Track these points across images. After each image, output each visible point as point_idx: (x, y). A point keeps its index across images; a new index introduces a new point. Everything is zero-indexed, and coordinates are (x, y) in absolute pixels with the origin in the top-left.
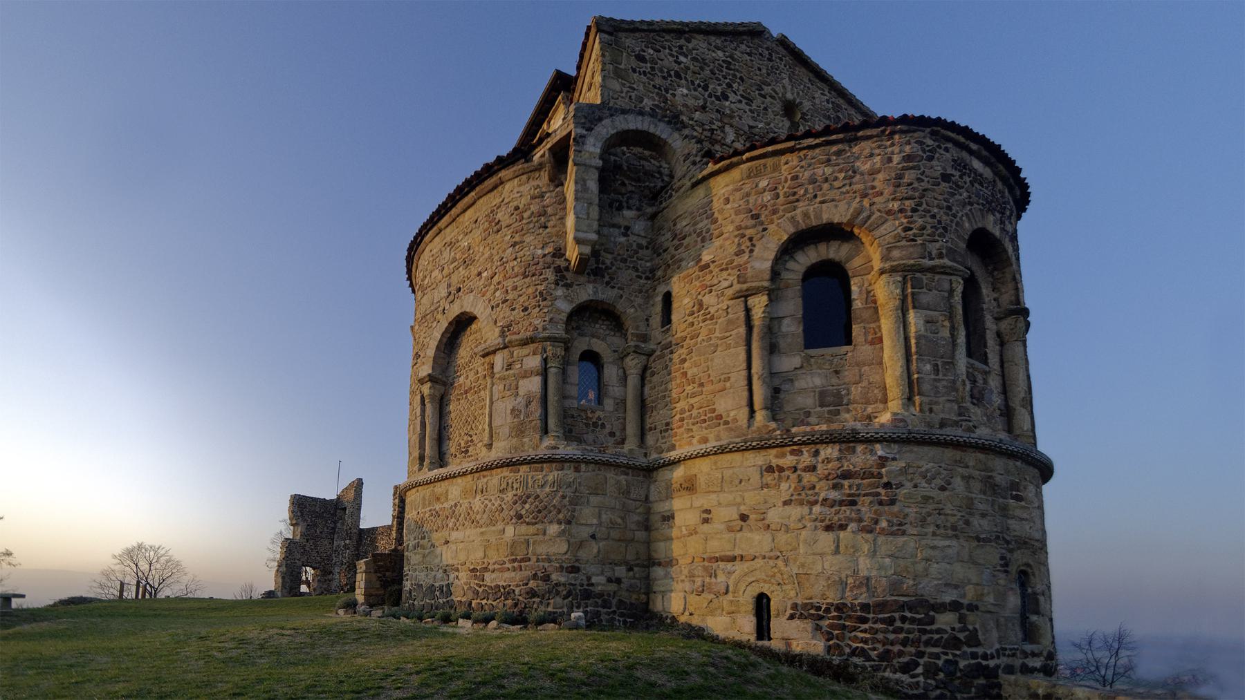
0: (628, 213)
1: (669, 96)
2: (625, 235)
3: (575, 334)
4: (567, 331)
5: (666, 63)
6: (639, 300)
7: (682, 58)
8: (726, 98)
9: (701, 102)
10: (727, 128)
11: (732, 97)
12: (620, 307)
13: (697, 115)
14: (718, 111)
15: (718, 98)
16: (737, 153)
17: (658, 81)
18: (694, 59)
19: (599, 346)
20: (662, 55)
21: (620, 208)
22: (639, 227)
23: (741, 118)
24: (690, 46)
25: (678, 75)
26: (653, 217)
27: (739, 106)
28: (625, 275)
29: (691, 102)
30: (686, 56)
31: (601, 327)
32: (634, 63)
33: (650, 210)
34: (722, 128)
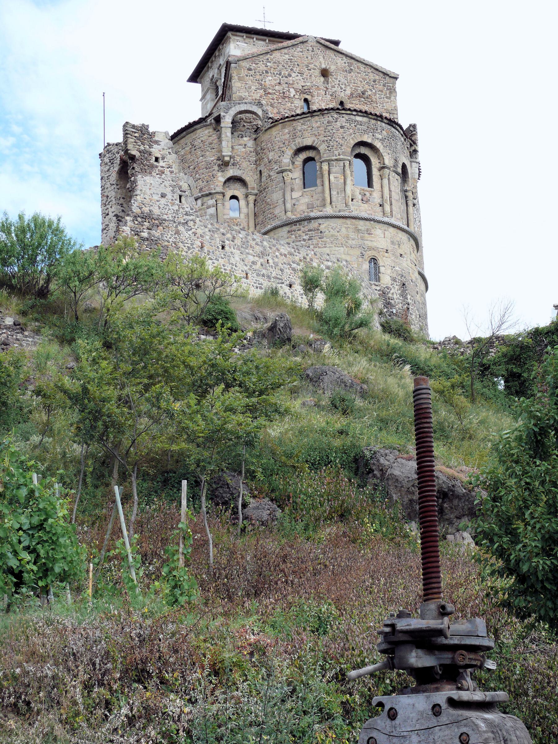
0: (245, 139)
1: (263, 83)
2: (244, 148)
3: (227, 189)
4: (223, 189)
5: (261, 68)
6: (251, 174)
7: (268, 64)
8: (290, 76)
9: (278, 81)
10: (292, 90)
11: (293, 75)
12: (244, 177)
13: (277, 88)
14: (286, 83)
15: (286, 77)
16: (276, 121)
17: (258, 77)
18: (275, 63)
19: (236, 193)
20: (259, 65)
21: (242, 137)
22: (251, 143)
23: (298, 83)
24: (272, 57)
25: (267, 72)
26: (255, 139)
27: (297, 78)
28: (245, 164)
29: (273, 83)
30: (270, 62)
31: (238, 185)
32: (246, 72)
33: (254, 136)
34: (289, 91)
